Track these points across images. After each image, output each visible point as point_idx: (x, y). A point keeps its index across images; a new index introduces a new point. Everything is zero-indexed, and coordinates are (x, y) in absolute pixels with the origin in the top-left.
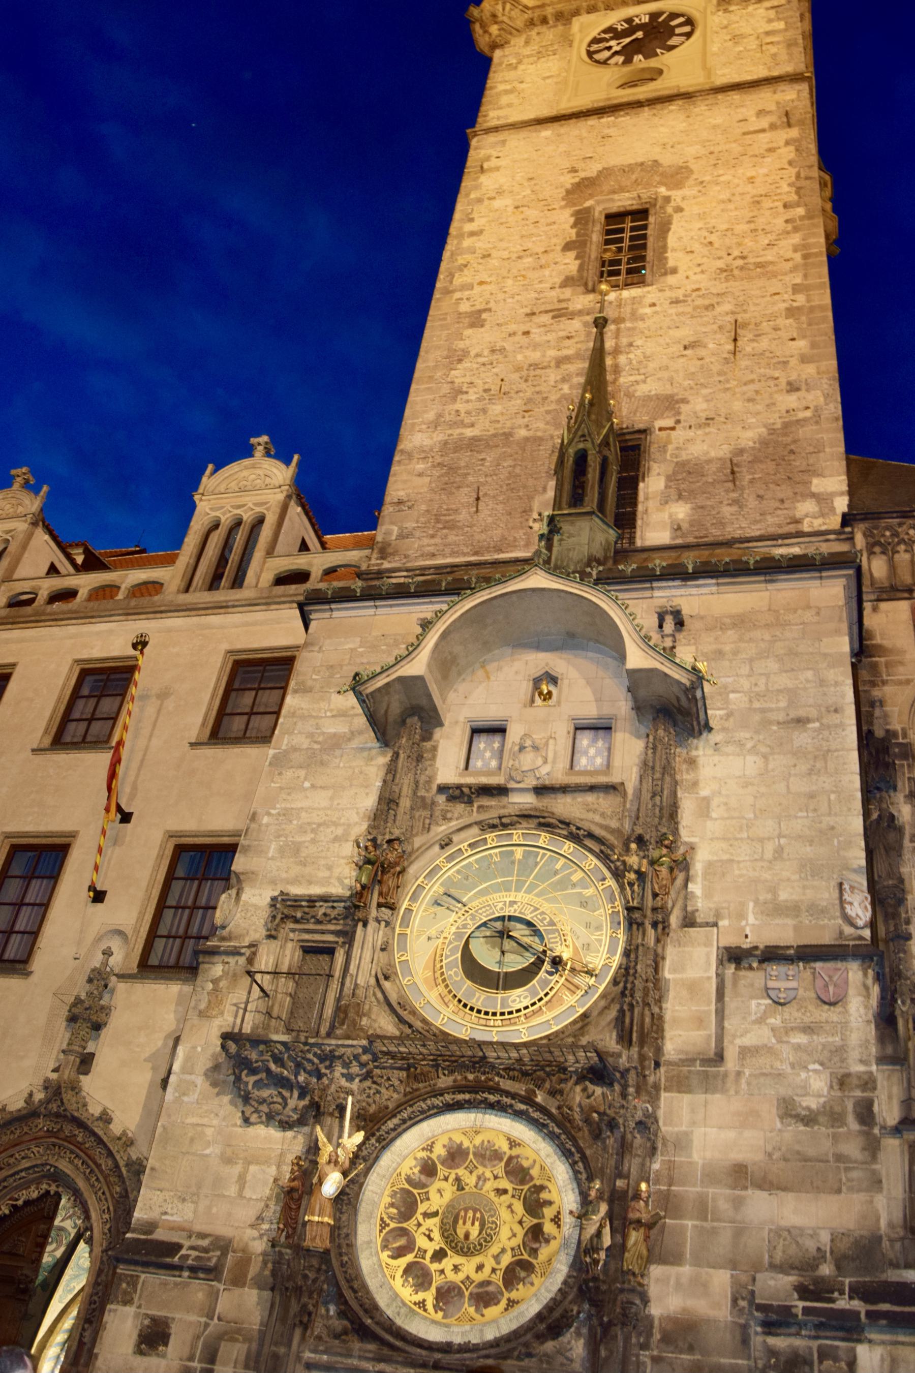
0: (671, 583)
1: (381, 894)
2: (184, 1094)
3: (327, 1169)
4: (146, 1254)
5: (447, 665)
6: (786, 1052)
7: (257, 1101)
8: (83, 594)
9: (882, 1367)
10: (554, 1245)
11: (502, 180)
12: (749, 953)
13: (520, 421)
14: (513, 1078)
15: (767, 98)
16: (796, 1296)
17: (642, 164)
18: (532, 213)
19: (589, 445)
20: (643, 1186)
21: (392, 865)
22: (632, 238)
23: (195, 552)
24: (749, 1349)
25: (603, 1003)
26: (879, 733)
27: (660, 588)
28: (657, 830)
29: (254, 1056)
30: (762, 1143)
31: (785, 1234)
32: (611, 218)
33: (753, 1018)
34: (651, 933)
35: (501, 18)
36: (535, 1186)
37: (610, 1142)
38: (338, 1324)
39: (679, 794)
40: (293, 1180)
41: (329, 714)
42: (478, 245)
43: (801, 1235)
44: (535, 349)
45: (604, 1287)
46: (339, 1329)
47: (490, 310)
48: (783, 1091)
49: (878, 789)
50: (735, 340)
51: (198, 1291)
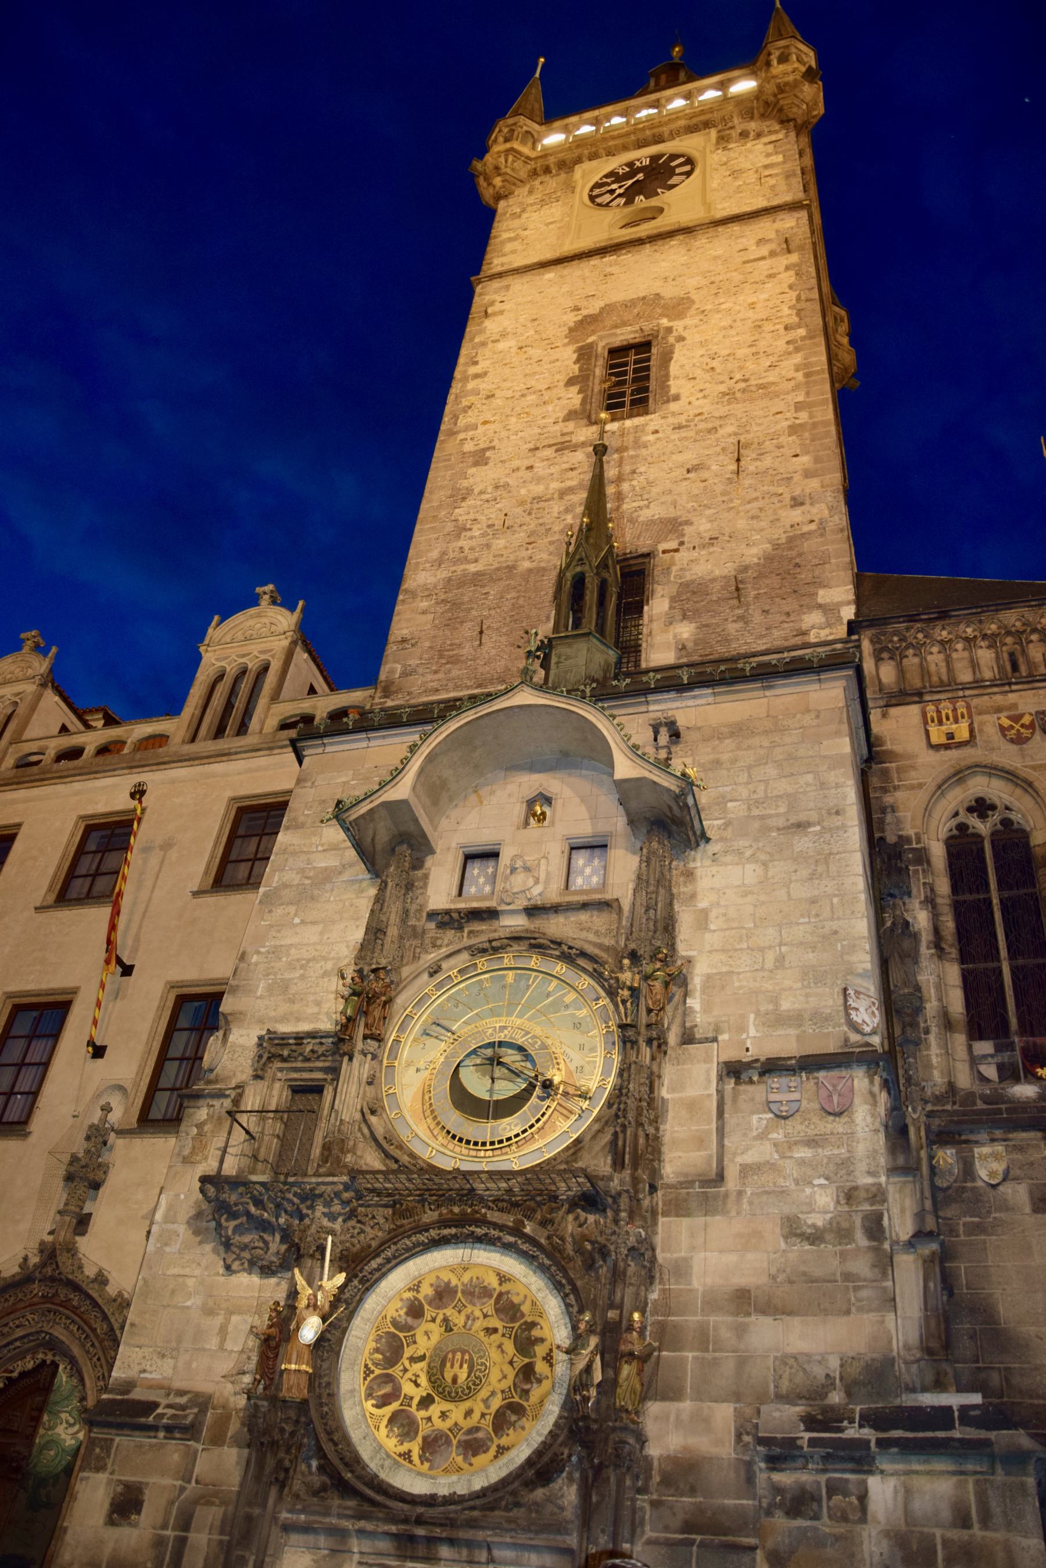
0: (666, 696)
1: (366, 1025)
2: (166, 1244)
3: (305, 1313)
4: (120, 1415)
5: (436, 789)
6: (790, 1168)
7: (238, 1247)
8: (90, 750)
9: (895, 1499)
10: (546, 1384)
11: (506, 323)
12: (749, 1065)
13: (524, 553)
14: (501, 1210)
15: (767, 228)
16: (802, 1427)
17: (644, 298)
18: (535, 353)
19: (587, 568)
20: (636, 1316)
21: (376, 996)
22: (635, 371)
23: (201, 702)
24: (754, 1487)
25: (597, 1127)
26: (891, 839)
27: (655, 702)
28: (651, 944)
29: (234, 1198)
30: (765, 1265)
31: (791, 1361)
32: (613, 352)
33: (755, 1134)
34: (646, 1052)
35: (504, 170)
36: (526, 1323)
37: (603, 1271)
38: (317, 1480)
39: (676, 907)
40: (270, 1327)
41: (320, 848)
42: (481, 386)
43: (809, 1362)
44: (538, 484)
45: (595, 1427)
46: (317, 1485)
47: (494, 448)
48: (787, 1210)
49: (892, 895)
50: (738, 460)
51: (174, 1452)
